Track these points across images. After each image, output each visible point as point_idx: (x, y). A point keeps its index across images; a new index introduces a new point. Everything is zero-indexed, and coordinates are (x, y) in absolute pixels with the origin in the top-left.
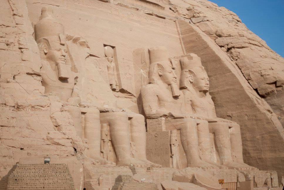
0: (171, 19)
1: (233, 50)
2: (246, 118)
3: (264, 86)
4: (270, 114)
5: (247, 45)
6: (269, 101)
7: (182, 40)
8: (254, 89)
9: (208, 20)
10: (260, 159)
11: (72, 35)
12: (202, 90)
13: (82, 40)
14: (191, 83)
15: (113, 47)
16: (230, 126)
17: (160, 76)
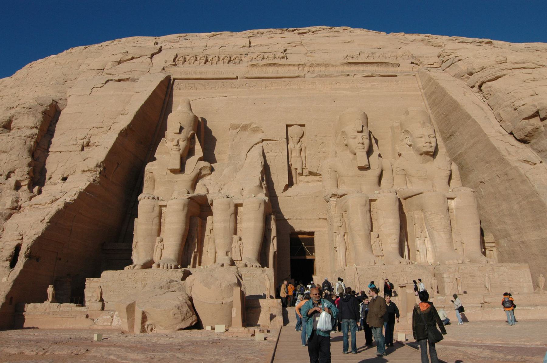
0: (408, 75)
1: (482, 88)
2: (498, 180)
3: (520, 124)
4: (532, 167)
5: (504, 72)
6: (535, 147)
7: (424, 96)
8: (509, 133)
9: (459, 60)
10: (523, 242)
11: (237, 122)
12: (421, 152)
13: (255, 126)
14: (410, 146)
15: (303, 126)
16: (453, 197)
17: (347, 145)
